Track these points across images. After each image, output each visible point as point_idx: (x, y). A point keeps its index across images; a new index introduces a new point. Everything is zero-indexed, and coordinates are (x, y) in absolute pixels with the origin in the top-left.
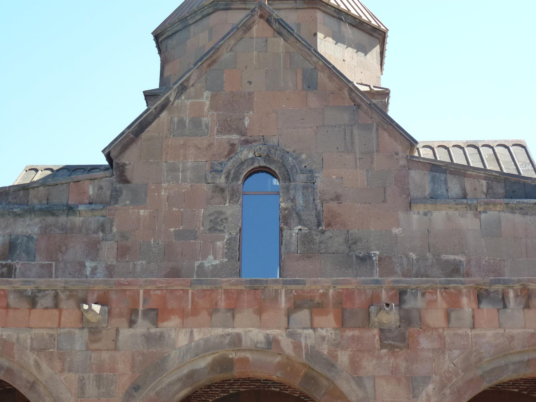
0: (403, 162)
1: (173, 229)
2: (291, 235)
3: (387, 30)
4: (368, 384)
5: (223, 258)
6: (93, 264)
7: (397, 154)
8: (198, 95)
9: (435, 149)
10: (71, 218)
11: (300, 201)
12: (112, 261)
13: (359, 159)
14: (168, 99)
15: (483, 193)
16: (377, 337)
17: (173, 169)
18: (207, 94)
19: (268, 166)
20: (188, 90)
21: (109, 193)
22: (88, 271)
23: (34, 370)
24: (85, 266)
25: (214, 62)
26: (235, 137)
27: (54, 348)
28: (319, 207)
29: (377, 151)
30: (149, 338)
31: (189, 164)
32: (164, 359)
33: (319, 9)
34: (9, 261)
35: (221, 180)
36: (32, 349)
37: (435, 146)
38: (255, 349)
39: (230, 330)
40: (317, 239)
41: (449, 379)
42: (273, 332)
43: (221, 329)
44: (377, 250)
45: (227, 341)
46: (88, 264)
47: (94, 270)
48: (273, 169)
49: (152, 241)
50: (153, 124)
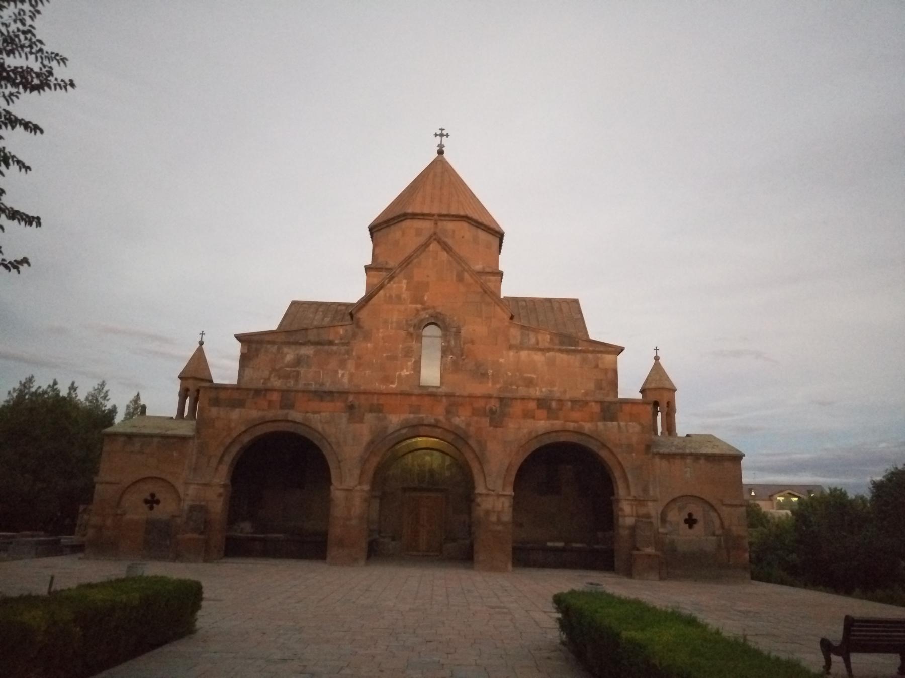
0: (507, 324)
1: (384, 355)
2: (447, 361)
5: (411, 371)
6: (343, 372)
7: (504, 319)
8: (400, 282)
11: (453, 342)
12: (353, 370)
14: (383, 283)
16: (488, 421)
17: (386, 322)
18: (405, 281)
19: (436, 322)
22: (340, 375)
24: (337, 372)
25: (408, 264)
26: (419, 306)
28: (462, 346)
31: (394, 320)
32: (386, 428)
33: (464, 221)
34: (297, 369)
35: (411, 330)
36: (321, 422)
40: (461, 362)
46: (340, 372)
47: (343, 375)
49: (374, 361)
50: (376, 296)
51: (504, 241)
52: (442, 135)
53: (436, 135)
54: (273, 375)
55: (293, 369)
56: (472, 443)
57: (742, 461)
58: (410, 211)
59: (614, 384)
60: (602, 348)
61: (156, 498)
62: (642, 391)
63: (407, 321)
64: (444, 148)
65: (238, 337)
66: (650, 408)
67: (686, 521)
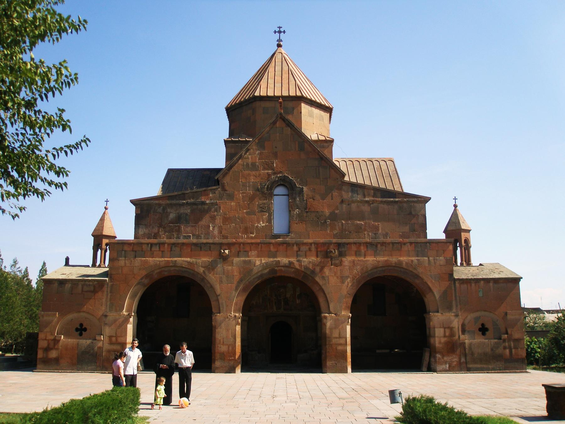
0: (340, 183)
3: (333, 108)
4: (326, 279)
7: (337, 179)
8: (255, 154)
9: (354, 162)
10: (203, 206)
13: (322, 181)
14: (242, 154)
15: (372, 196)
19: (284, 184)
20: (250, 151)
21: (218, 195)
23: (204, 275)
27: (210, 266)
29: (329, 178)
30: (245, 262)
32: (252, 270)
33: (303, 101)
36: (202, 267)
37: (353, 160)
38: (285, 266)
39: (276, 259)
41: (355, 277)
42: (292, 260)
43: (272, 259)
44: (329, 220)
45: (274, 263)
48: (286, 185)
49: (237, 215)
51: (333, 114)
52: (280, 32)
53: (275, 32)
54: (160, 230)
55: (176, 225)
56: (317, 279)
57: (520, 283)
58: (257, 94)
59: (423, 226)
60: (414, 199)
61: (83, 328)
62: (445, 231)
63: (261, 184)
64: (281, 43)
65: (132, 202)
66: (451, 247)
67: (480, 330)
